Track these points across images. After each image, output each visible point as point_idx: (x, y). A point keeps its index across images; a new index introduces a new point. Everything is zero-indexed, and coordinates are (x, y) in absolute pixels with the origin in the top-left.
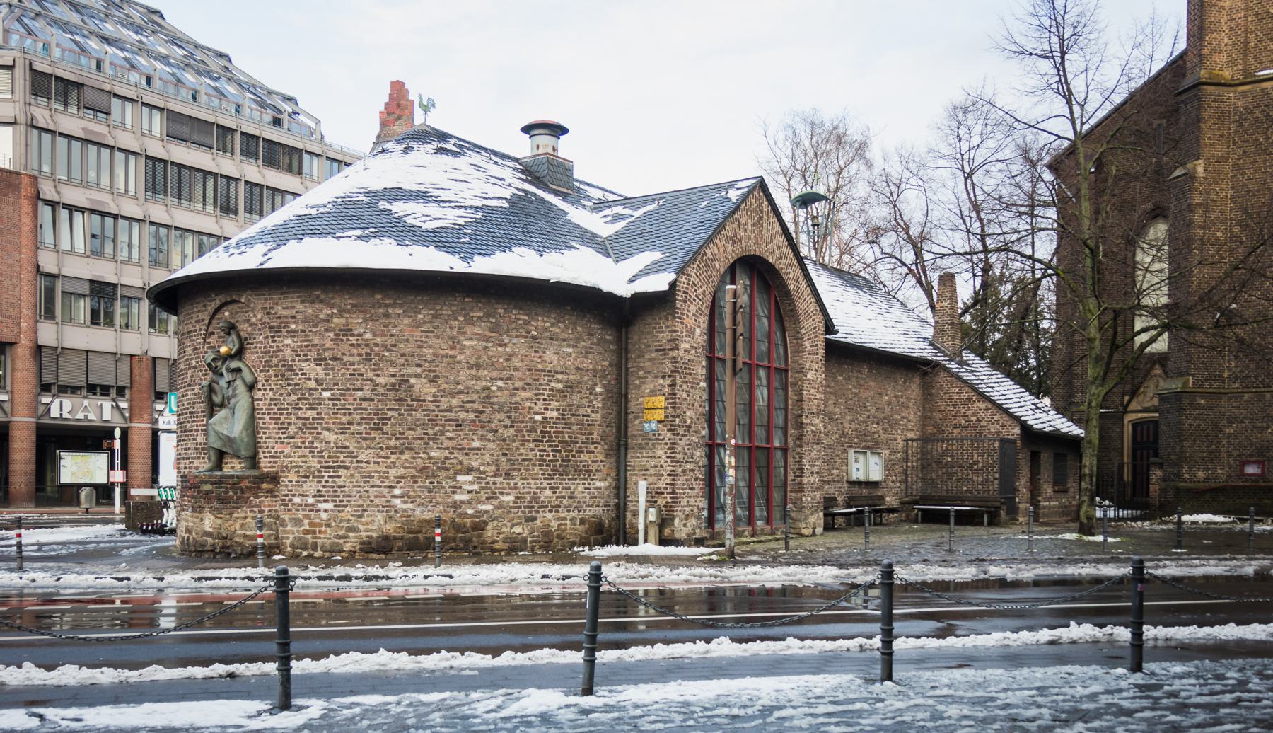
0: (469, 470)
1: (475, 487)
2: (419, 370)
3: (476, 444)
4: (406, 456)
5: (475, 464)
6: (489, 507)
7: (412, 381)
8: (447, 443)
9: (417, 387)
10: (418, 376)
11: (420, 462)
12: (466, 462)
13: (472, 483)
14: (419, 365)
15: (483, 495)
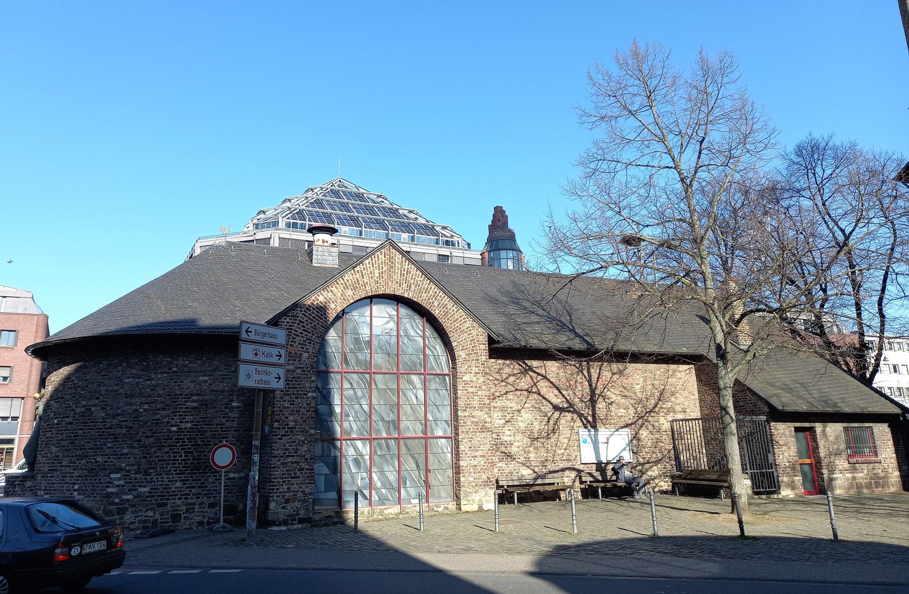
0: (118, 470)
1: (122, 482)
2: (97, 401)
3: (125, 451)
4: (83, 462)
5: (123, 465)
6: (131, 497)
7: (93, 409)
8: (107, 451)
9: (95, 412)
10: (96, 405)
11: (90, 465)
12: (118, 464)
13: (120, 479)
14: (97, 398)
15: (127, 488)
